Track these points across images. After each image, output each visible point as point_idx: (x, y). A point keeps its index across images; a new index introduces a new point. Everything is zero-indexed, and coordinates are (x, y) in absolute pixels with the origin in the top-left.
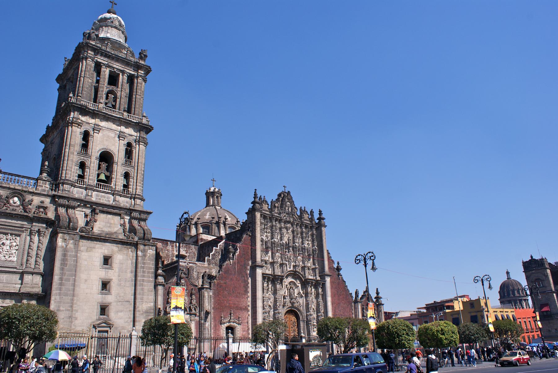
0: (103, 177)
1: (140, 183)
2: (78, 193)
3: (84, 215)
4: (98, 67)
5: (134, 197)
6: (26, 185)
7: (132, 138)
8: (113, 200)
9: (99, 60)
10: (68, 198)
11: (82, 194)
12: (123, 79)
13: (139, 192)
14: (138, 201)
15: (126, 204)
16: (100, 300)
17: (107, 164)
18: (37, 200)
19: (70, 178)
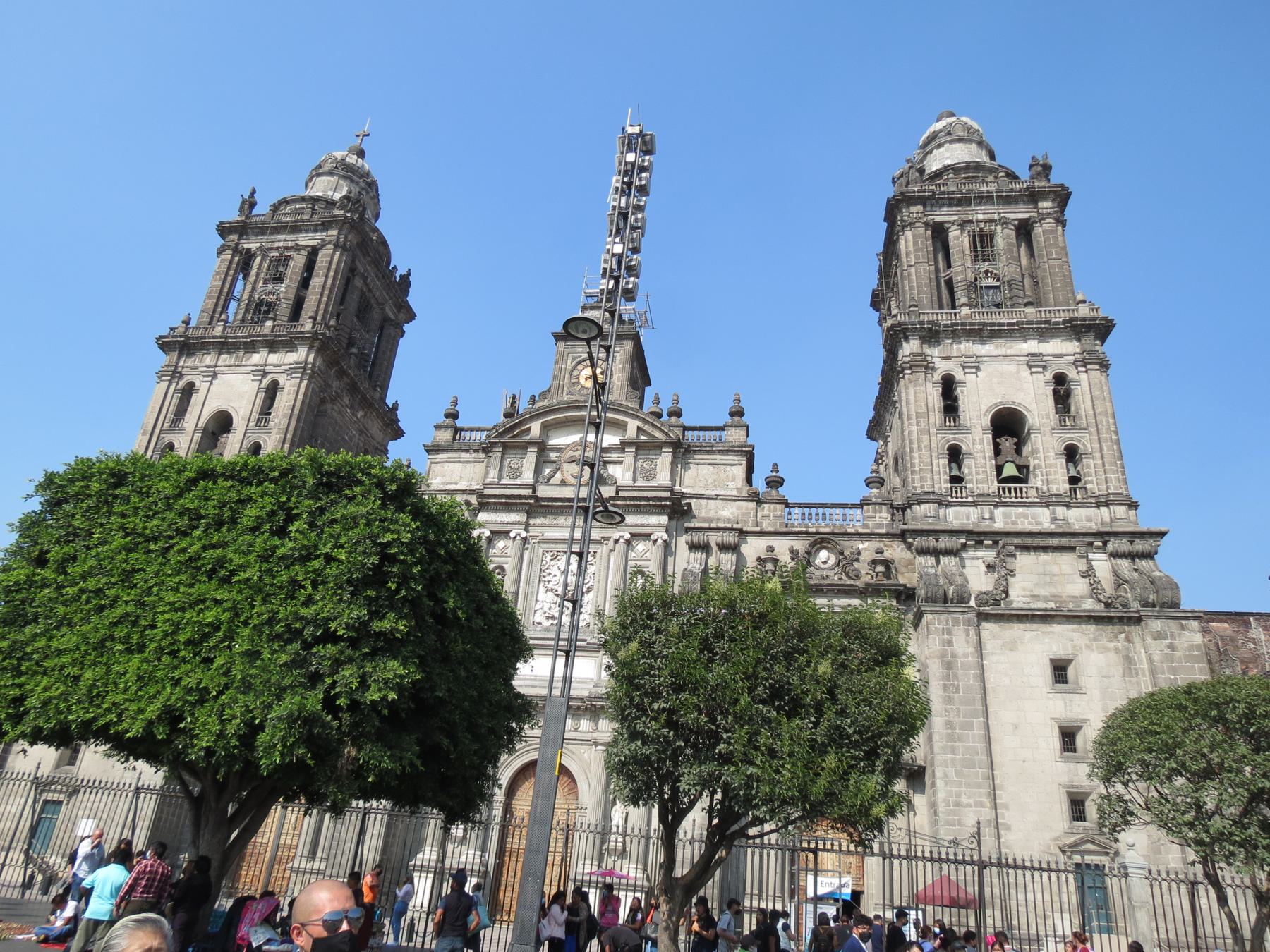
0: (1010, 470)
1: (1111, 464)
2: (957, 517)
3: (983, 568)
4: (939, 233)
5: (1106, 502)
6: (841, 522)
7: (1062, 361)
8: (1049, 520)
9: (938, 219)
10: (936, 533)
11: (968, 518)
12: (1003, 239)
13: (1116, 488)
14: (1120, 511)
15: (1089, 524)
16: (1065, 779)
17: (1015, 440)
18: (867, 548)
19: (933, 486)
